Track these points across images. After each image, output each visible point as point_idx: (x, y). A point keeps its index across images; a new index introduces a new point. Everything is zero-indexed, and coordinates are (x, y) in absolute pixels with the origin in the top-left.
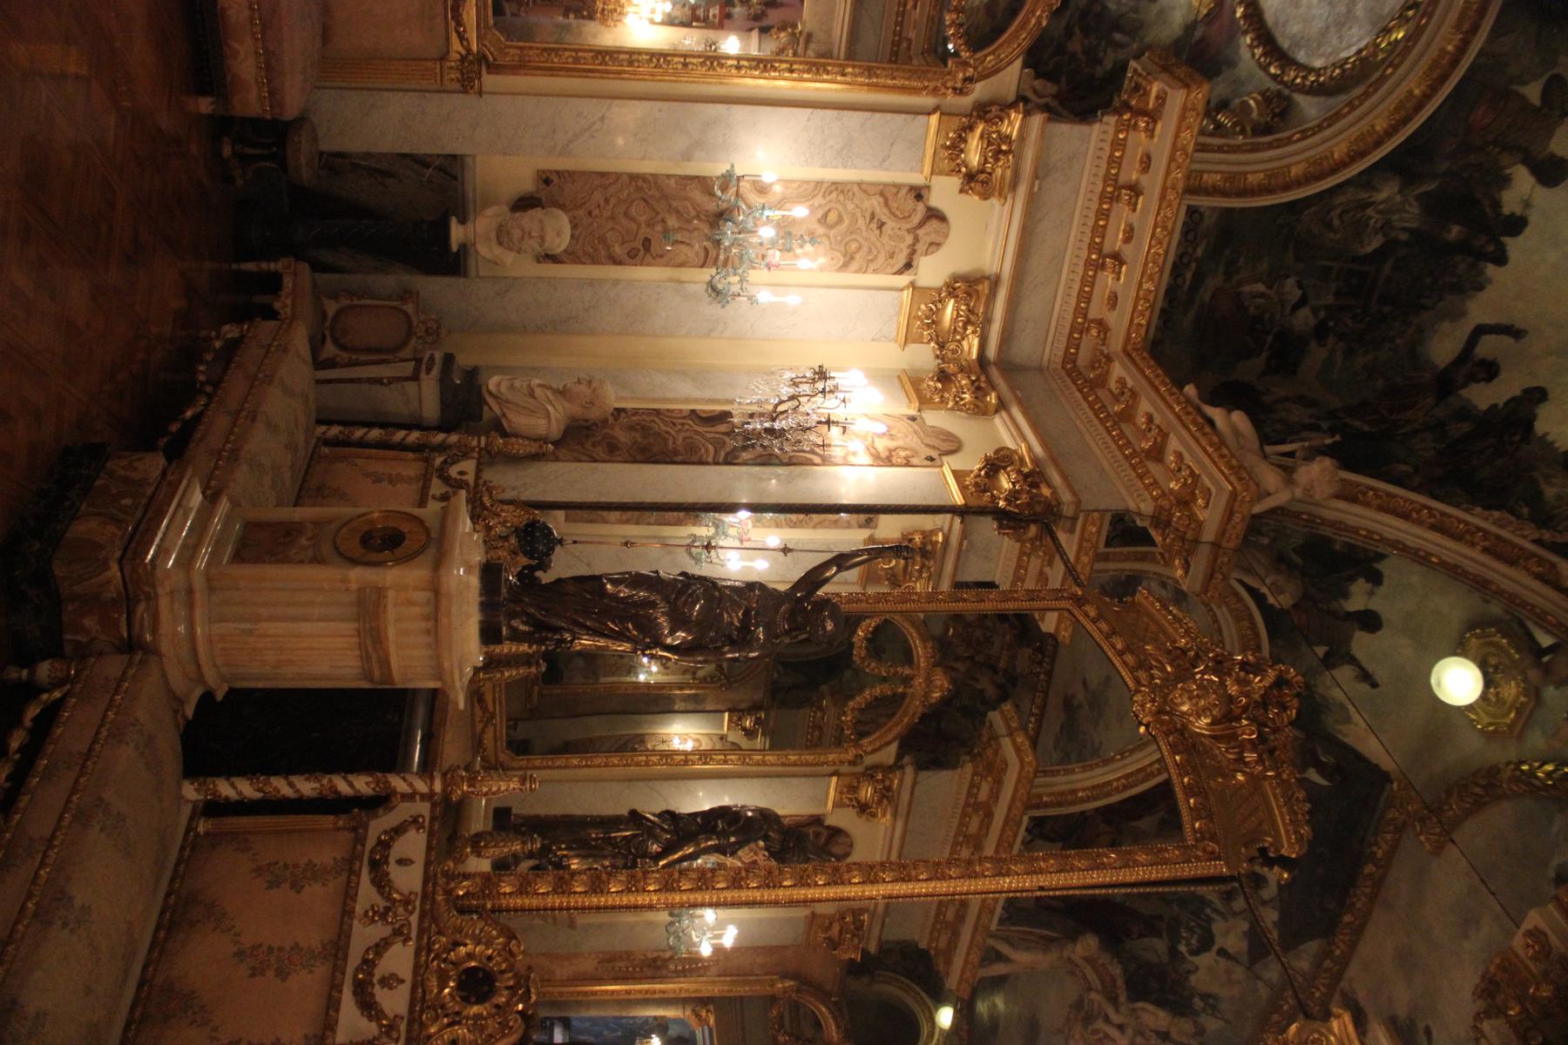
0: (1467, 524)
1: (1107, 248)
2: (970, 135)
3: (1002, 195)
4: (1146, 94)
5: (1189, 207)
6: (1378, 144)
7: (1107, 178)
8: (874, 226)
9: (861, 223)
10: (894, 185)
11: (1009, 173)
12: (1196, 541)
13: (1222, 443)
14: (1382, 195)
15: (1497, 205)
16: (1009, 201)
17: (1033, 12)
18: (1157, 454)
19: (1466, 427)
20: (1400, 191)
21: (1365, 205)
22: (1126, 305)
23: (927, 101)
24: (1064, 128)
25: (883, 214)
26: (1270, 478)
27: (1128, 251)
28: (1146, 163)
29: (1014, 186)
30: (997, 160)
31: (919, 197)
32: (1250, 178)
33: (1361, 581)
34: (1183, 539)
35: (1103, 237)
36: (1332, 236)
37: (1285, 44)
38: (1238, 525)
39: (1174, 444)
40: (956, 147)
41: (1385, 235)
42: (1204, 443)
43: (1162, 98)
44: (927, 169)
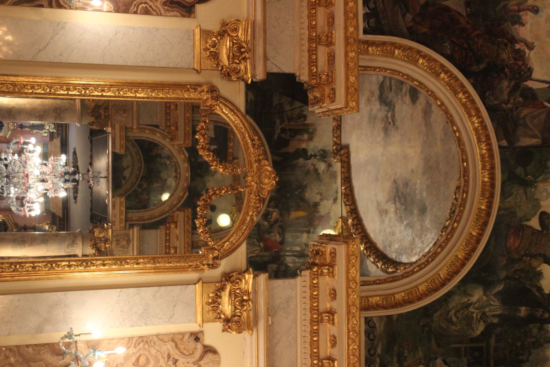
1: (322, 354)
2: (223, 294)
3: (250, 328)
4: (323, 254)
5: (366, 318)
6: (463, 265)
7: (312, 309)
8: (171, 363)
9: (162, 362)
10: (180, 334)
11: (251, 314)
14: (474, 299)
15: (540, 289)
16: (255, 330)
17: (247, 213)
20: (485, 294)
21: (468, 306)
22: (343, 341)
23: (193, 276)
24: (279, 283)
25: (175, 354)
27: (335, 352)
28: (333, 294)
29: (256, 323)
30: (243, 306)
31: (197, 339)
32: (397, 296)
35: (318, 348)
36: (454, 327)
37: (393, 256)
40: (215, 303)
41: (484, 322)
43: (333, 254)
44: (199, 319)
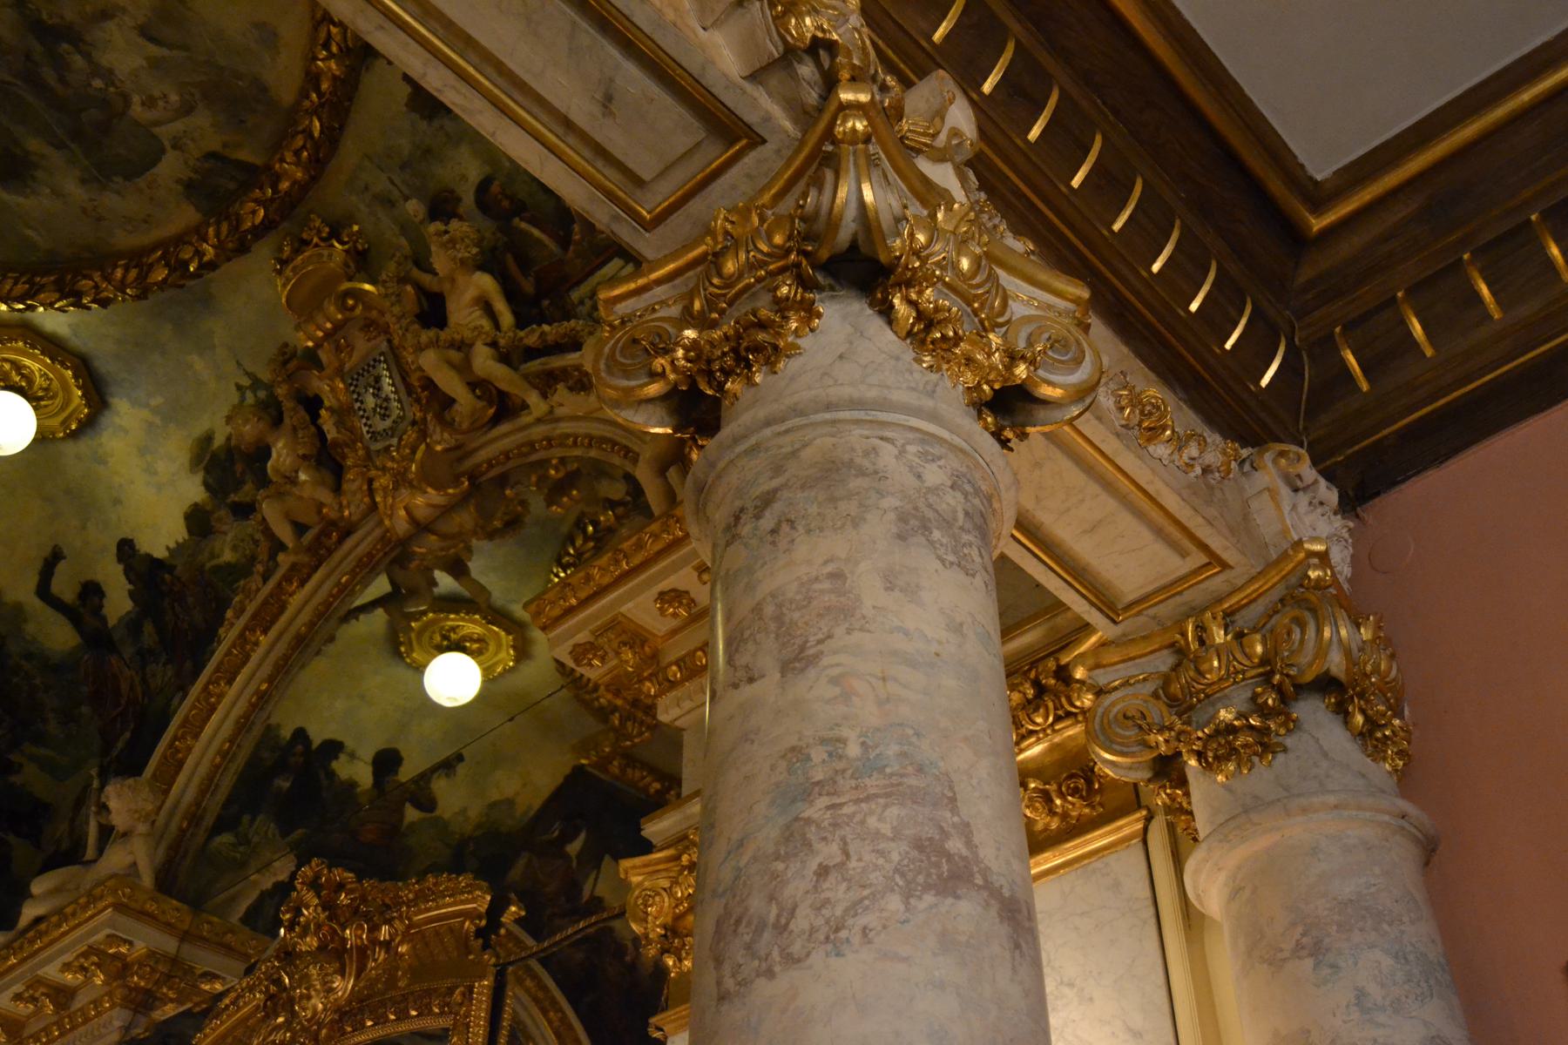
0: (234, 646)
12: (175, 961)
13: (59, 911)
18: (62, 995)
19: (148, 628)
26: (116, 859)
33: (335, 765)
34: (169, 977)
38: (172, 909)
39: (51, 972)
42: (56, 934)
